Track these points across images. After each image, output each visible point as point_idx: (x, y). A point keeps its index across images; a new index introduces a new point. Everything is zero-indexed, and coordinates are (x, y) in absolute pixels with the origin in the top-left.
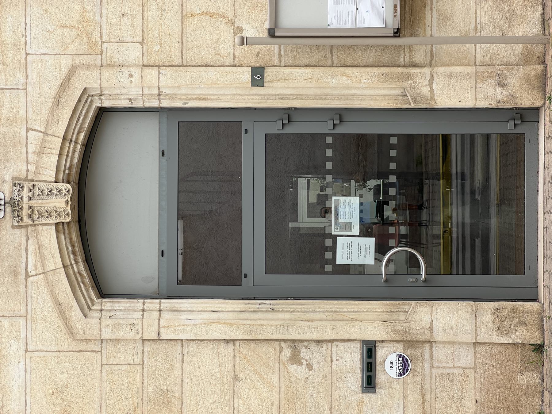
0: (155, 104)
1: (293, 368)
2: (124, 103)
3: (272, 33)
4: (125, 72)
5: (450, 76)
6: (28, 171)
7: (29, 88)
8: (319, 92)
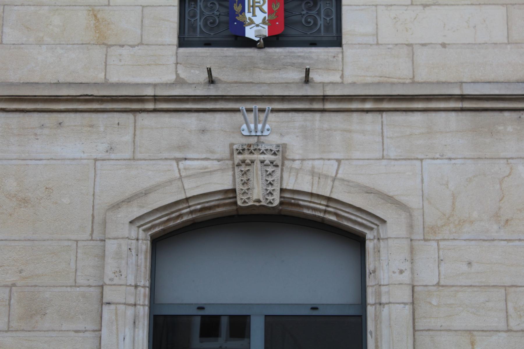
0: (370, 299)
2: (370, 264)
4: (406, 266)
6: (294, 160)
7: (384, 162)
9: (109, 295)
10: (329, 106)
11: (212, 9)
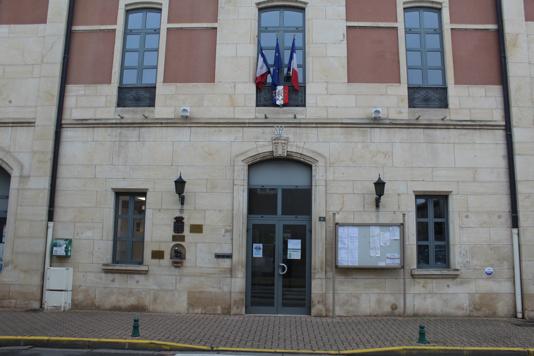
0: (313, 184)
1: (223, 230)
2: (313, 174)
3: (337, 224)
4: (324, 174)
5: (322, 285)
8: (317, 240)
9: (236, 183)
10: (301, 126)
11: (266, 95)
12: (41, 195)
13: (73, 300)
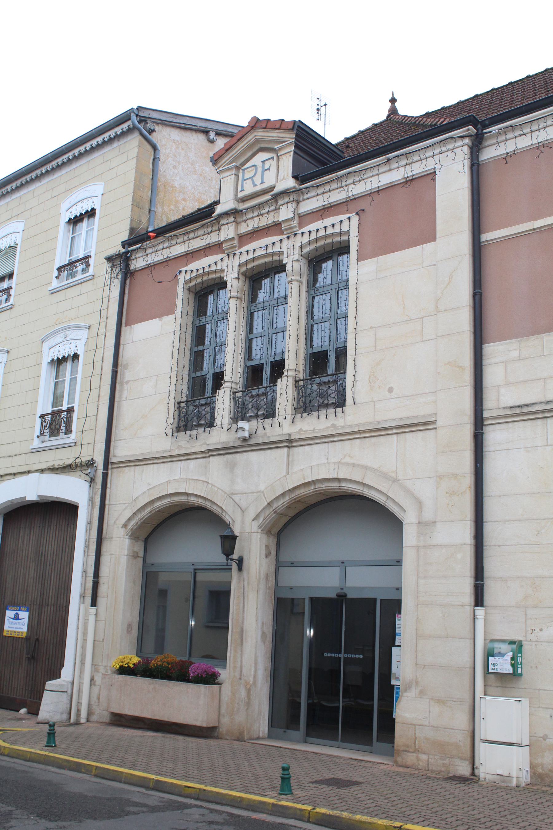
12: (459, 556)
13: (532, 766)
